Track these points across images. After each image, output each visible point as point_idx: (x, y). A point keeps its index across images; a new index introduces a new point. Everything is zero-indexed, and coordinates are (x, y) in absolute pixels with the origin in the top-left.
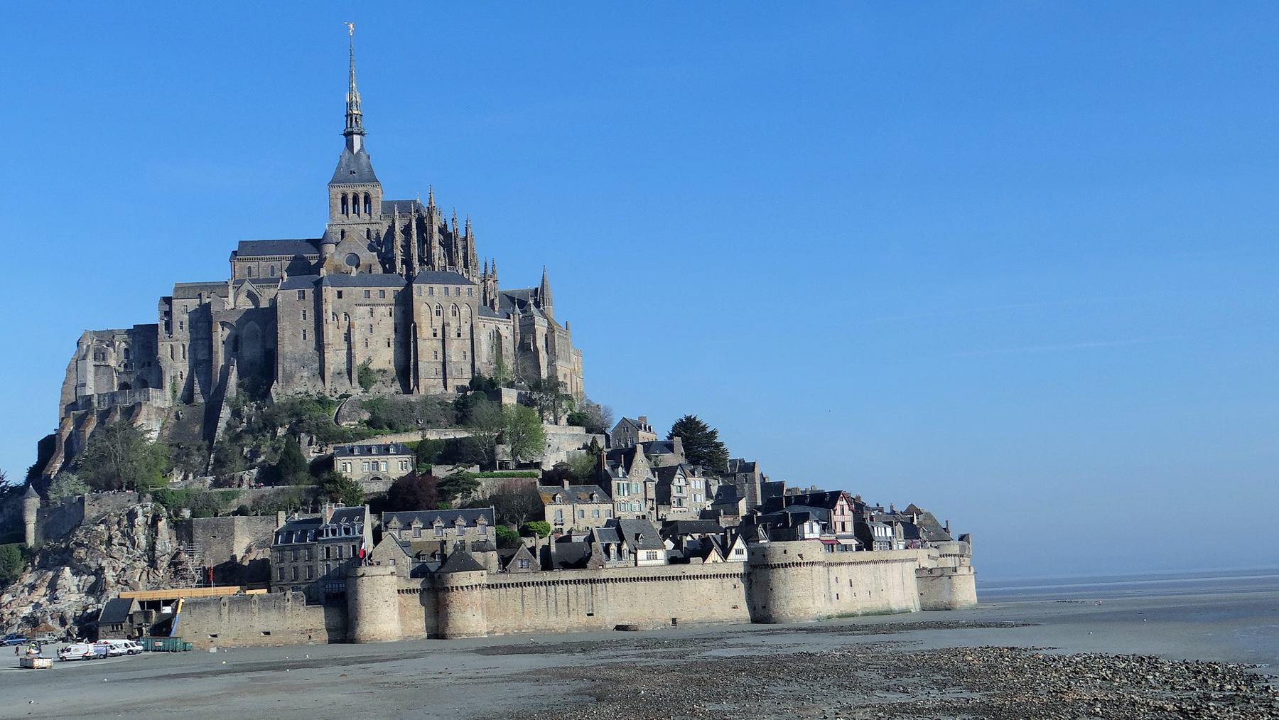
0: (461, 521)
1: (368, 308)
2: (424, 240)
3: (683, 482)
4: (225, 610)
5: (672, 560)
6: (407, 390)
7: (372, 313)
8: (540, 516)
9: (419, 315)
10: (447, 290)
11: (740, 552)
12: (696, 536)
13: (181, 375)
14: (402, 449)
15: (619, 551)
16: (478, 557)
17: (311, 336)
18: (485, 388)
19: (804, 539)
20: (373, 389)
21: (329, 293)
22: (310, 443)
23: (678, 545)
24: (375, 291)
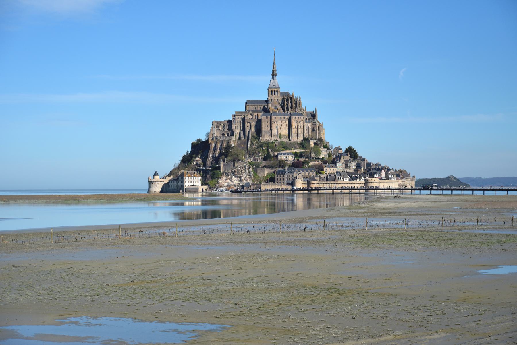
0: (309, 171)
1: (281, 121)
2: (291, 103)
3: (350, 164)
4: (271, 186)
5: (350, 180)
6: (290, 140)
7: (282, 122)
8: (323, 170)
9: (292, 123)
10: (298, 117)
11: (363, 179)
12: (353, 175)
13: (237, 133)
14: (292, 154)
15: (340, 178)
16: (316, 178)
17: (269, 127)
18: (306, 140)
19: (375, 177)
20: (282, 139)
21: (273, 117)
22: (271, 152)
23: (351, 177)
24: (282, 117)
